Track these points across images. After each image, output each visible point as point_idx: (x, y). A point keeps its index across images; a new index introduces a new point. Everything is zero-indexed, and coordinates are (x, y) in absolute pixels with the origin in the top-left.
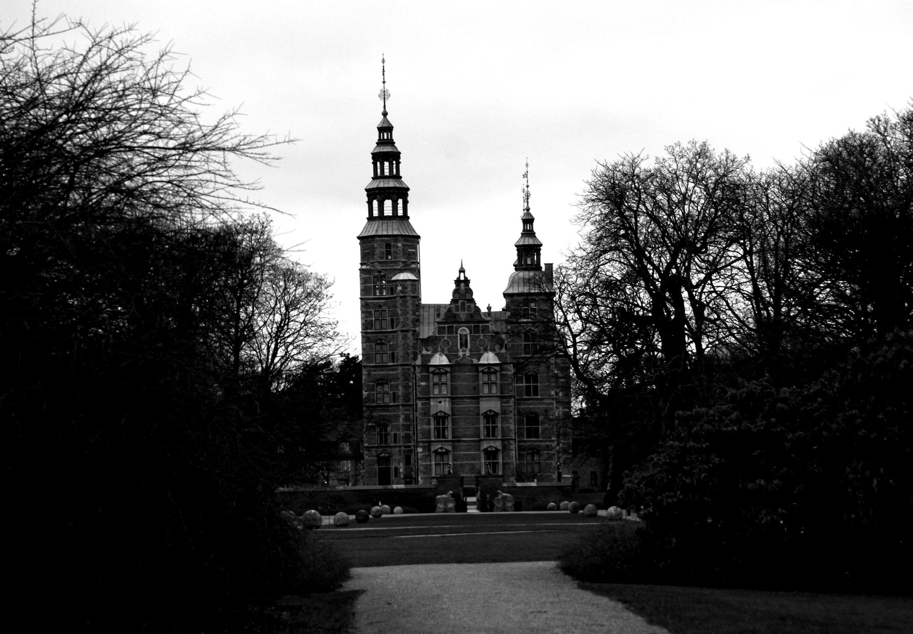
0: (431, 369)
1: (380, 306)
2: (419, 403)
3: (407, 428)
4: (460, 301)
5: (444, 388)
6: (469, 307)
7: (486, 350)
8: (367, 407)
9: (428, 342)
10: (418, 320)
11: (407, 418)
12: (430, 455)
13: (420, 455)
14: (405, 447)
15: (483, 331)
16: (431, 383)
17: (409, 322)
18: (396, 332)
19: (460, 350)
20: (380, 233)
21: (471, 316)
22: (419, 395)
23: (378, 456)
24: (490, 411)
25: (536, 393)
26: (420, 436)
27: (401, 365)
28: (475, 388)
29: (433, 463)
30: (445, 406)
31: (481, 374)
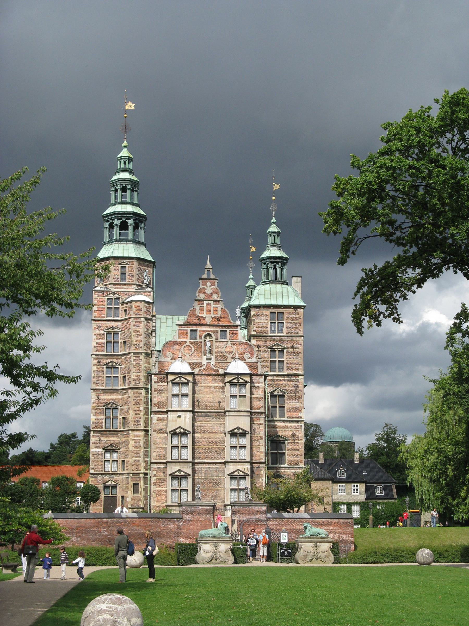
0: (170, 378)
1: (113, 328)
2: (155, 417)
3: (136, 454)
4: (205, 303)
5: (185, 400)
6: (216, 310)
7: (234, 358)
8: (94, 431)
9: (170, 345)
10: (154, 331)
11: (136, 444)
12: (165, 480)
13: (153, 479)
14: (134, 474)
15: (231, 337)
16: (170, 394)
17: (142, 344)
18: (129, 354)
19: (204, 358)
20: (115, 255)
21: (218, 320)
22: (155, 409)
23: (104, 484)
24: (238, 428)
25: (282, 415)
26: (154, 456)
27: (132, 388)
28: (219, 402)
29: (169, 488)
30: (186, 422)
31: (228, 385)
